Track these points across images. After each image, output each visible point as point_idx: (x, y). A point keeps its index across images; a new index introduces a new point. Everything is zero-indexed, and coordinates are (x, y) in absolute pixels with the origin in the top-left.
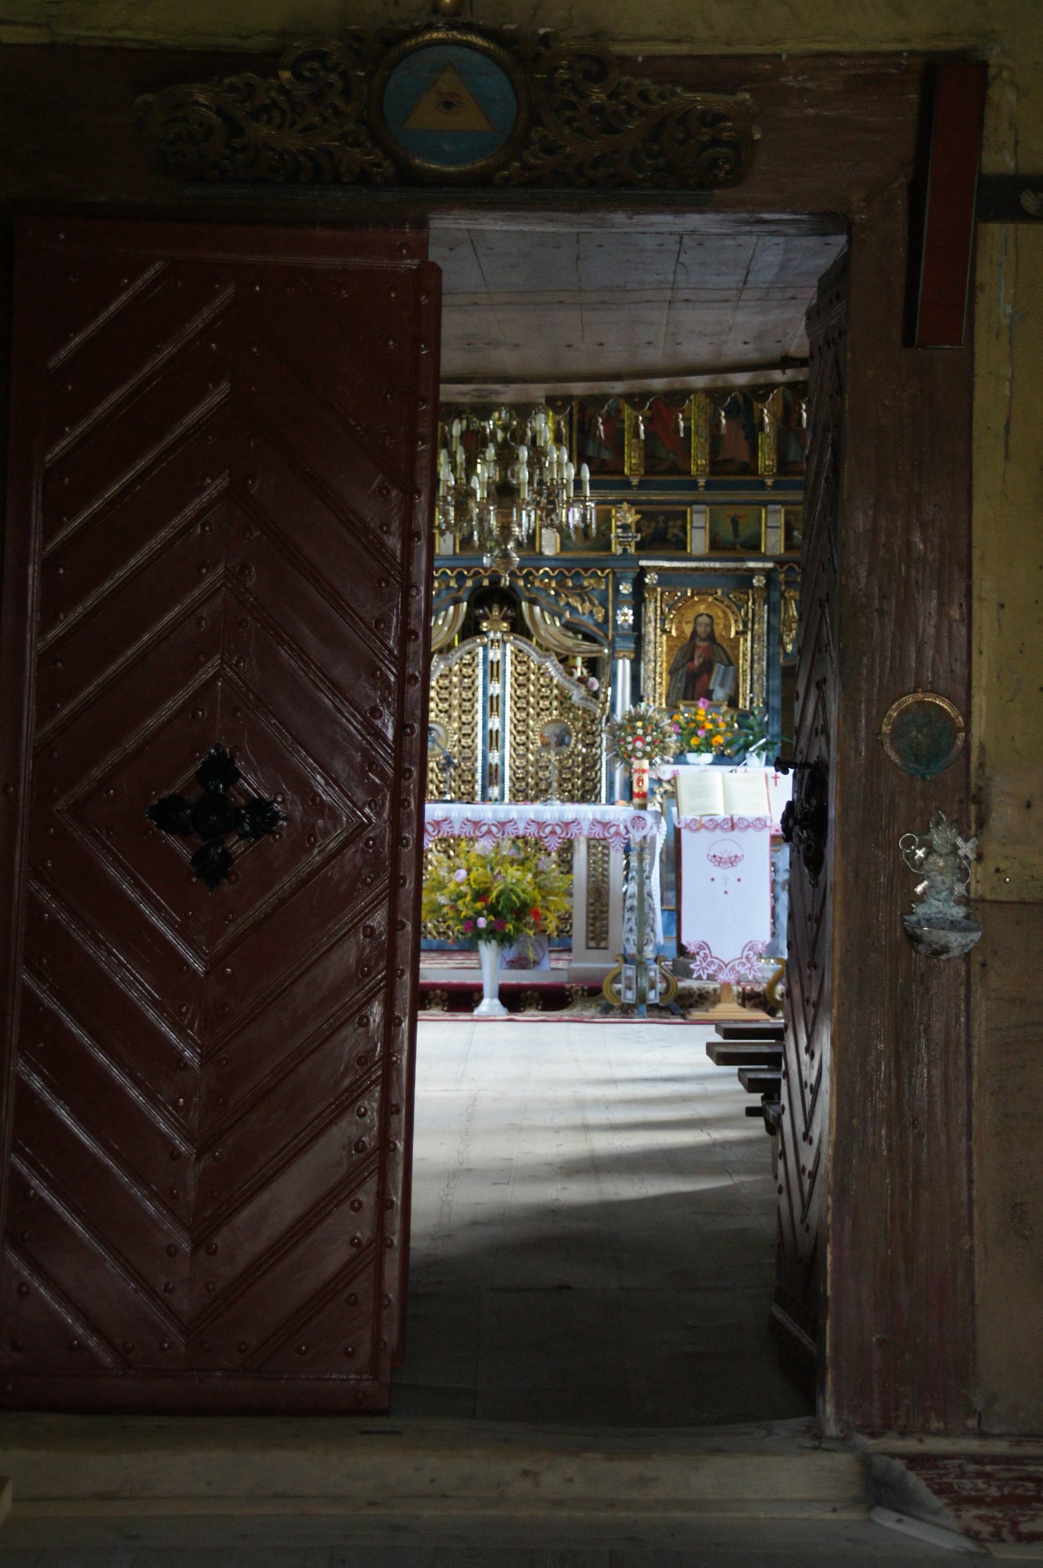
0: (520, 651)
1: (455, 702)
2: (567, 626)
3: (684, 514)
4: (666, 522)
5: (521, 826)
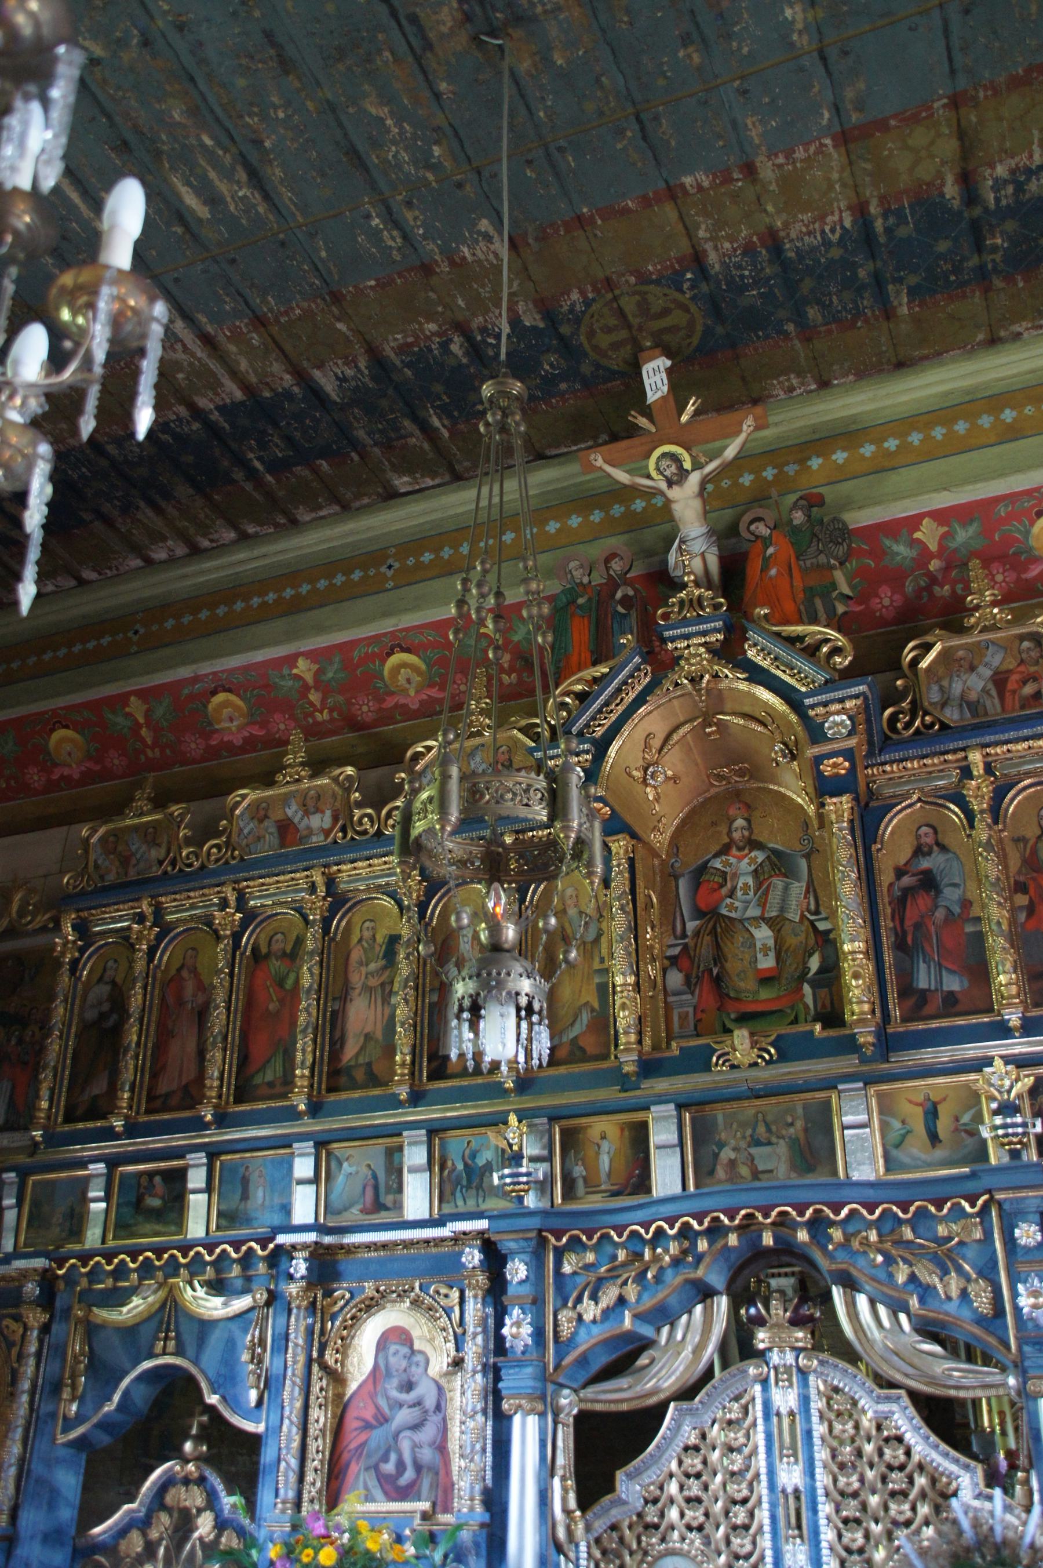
0: (836, 1390)
2: (928, 1330)
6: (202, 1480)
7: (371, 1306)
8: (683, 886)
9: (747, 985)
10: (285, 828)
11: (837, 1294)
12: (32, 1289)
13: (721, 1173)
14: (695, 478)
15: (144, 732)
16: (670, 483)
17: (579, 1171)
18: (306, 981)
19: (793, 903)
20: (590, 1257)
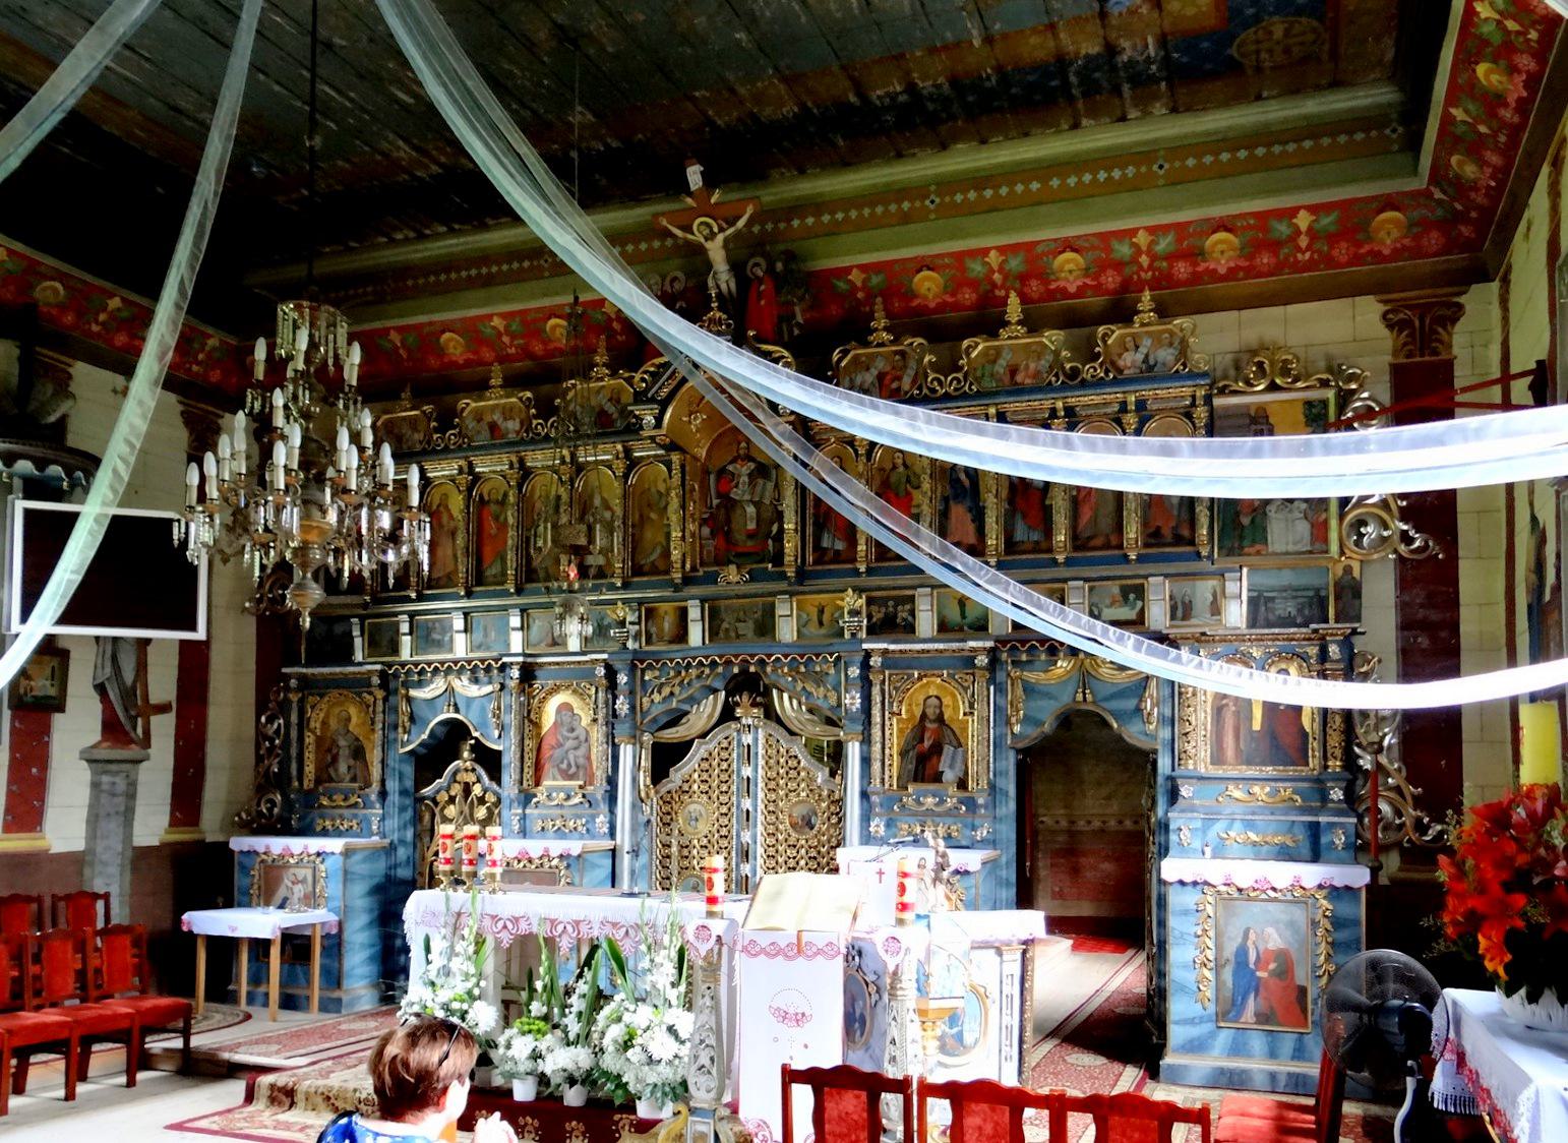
1: (715, 784)
3: (912, 599)
4: (895, 607)
5: (596, 926)
6: (473, 770)
7: (555, 690)
8: (712, 478)
9: (740, 537)
10: (493, 428)
11: (775, 692)
12: (376, 680)
13: (722, 635)
14: (720, 237)
15: (401, 351)
16: (706, 239)
17: (653, 630)
18: (511, 520)
19: (767, 494)
20: (657, 673)
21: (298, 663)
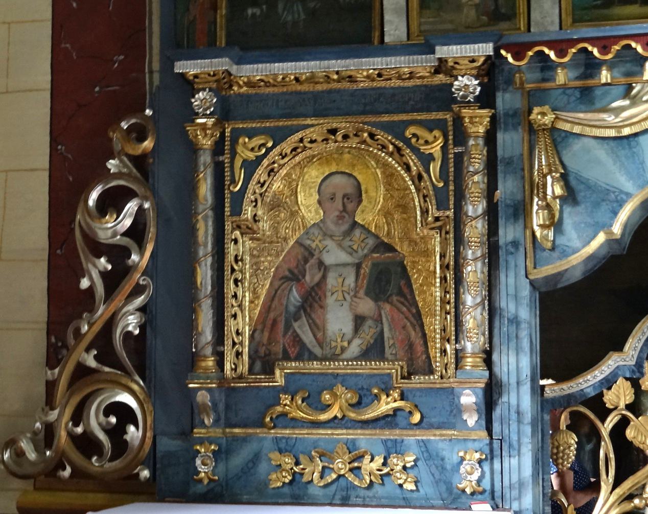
21: (210, 49)
